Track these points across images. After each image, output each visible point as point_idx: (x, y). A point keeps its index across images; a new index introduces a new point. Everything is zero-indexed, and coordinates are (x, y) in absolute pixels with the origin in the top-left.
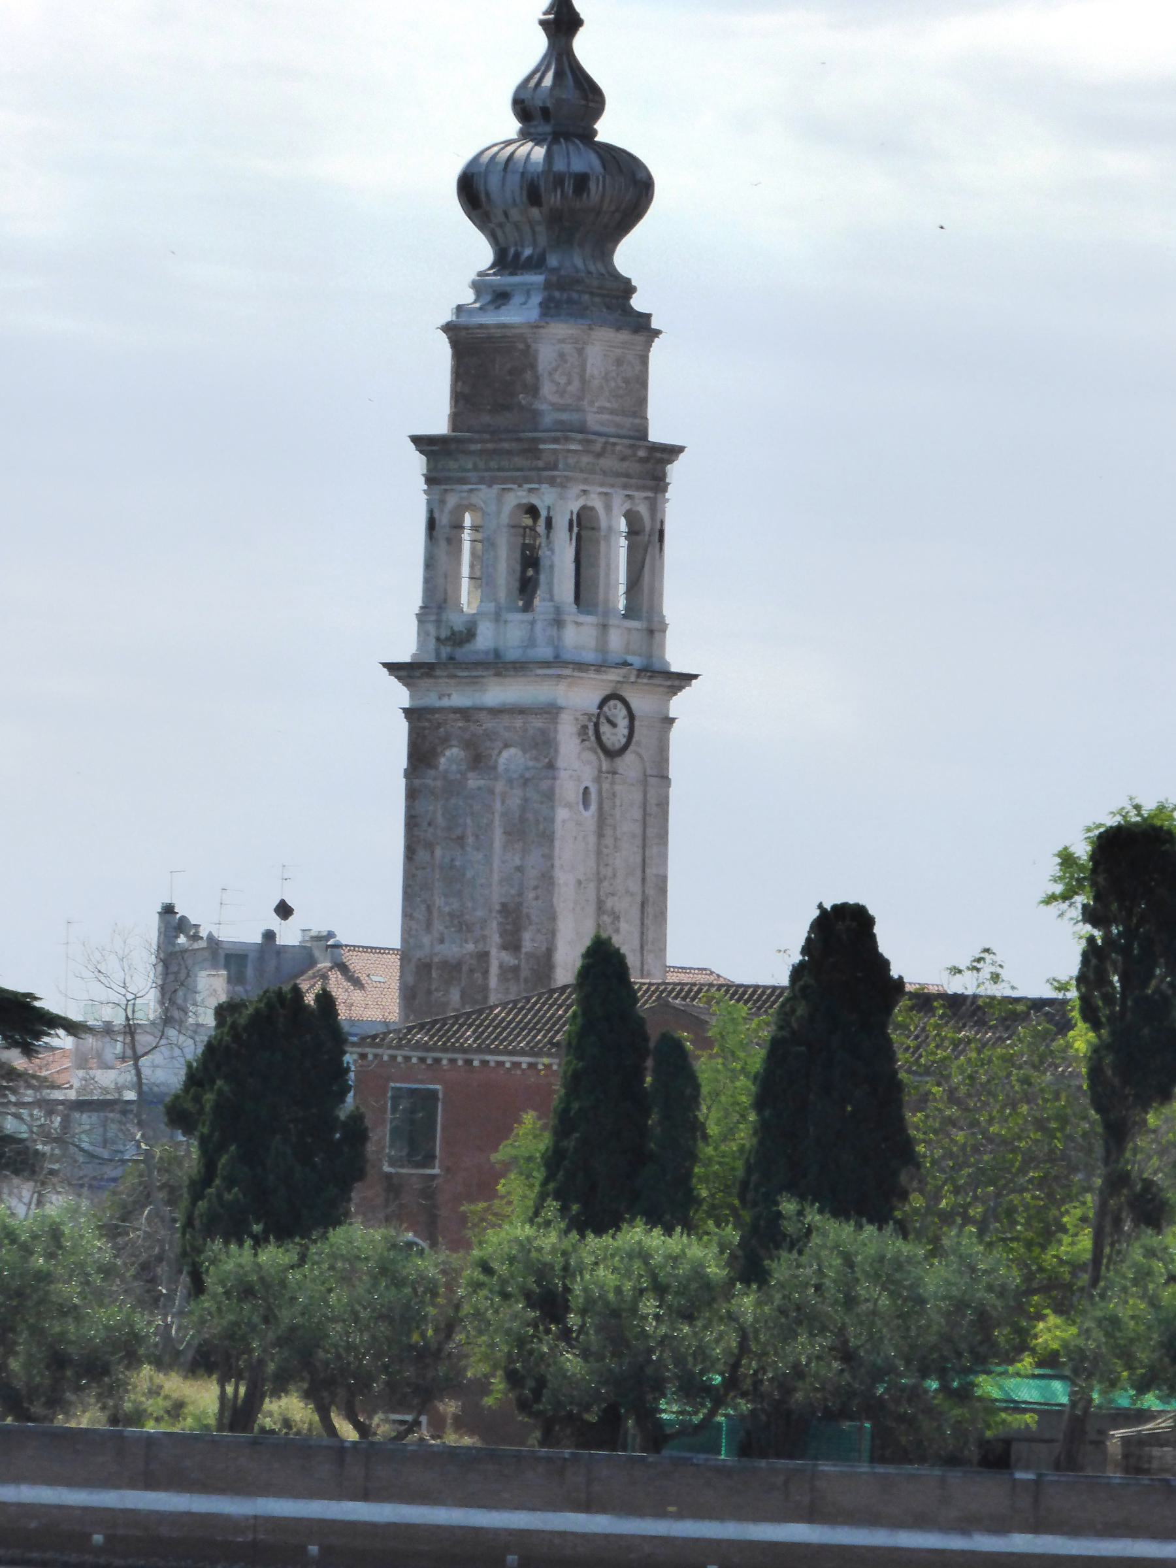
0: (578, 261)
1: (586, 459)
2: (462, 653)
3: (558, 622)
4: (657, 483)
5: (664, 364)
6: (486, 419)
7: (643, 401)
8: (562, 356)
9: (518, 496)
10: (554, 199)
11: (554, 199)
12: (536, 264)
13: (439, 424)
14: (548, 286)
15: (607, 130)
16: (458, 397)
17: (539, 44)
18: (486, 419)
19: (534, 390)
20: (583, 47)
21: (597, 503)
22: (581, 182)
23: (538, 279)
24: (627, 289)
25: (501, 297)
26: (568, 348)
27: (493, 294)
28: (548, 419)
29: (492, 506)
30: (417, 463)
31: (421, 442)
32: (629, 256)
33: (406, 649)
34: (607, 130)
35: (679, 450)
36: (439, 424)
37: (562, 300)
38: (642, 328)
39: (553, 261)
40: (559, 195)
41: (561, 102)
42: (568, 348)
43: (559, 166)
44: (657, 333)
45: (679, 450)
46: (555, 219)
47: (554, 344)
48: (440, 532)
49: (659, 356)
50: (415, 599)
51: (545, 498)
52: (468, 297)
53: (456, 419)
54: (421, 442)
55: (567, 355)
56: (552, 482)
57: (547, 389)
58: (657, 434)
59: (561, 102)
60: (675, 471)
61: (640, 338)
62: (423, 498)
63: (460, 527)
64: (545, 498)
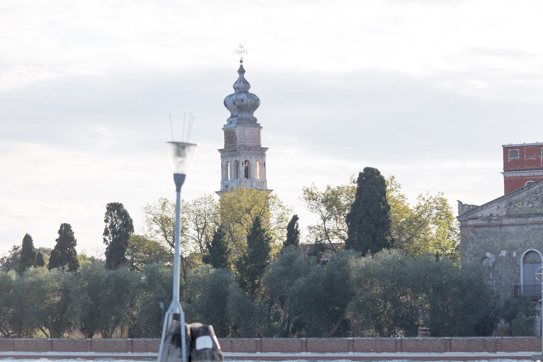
0: (244, 115)
1: (245, 151)
2: (228, 189)
5: (263, 133)
6: (229, 145)
7: (259, 140)
8: (240, 133)
9: (234, 159)
10: (238, 104)
11: (238, 104)
12: (237, 116)
13: (223, 147)
14: (238, 120)
15: (250, 91)
16: (226, 142)
17: (237, 76)
18: (229, 145)
19: (236, 139)
20: (246, 76)
21: (250, 159)
22: (242, 100)
23: (236, 119)
24: (255, 120)
25: (231, 122)
26: (241, 131)
27: (230, 122)
28: (238, 144)
30: (219, 154)
31: (220, 150)
32: (256, 114)
33: (219, 189)
34: (250, 91)
35: (268, 148)
36: (223, 147)
37: (241, 122)
38: (259, 127)
39: (239, 115)
40: (243, 104)
41: (242, 86)
42: (241, 131)
43: (238, 97)
44: (261, 127)
45: (268, 148)
46: (239, 107)
47: (238, 131)
48: (224, 168)
49: (262, 132)
50: (220, 179)
51: (238, 158)
52: (226, 123)
54: (220, 150)
55: (242, 133)
56: (239, 156)
57: (238, 139)
58: (263, 145)
59: (242, 86)
60: (267, 153)
61: (257, 129)
62: (220, 161)
63: (228, 166)
64: (238, 158)
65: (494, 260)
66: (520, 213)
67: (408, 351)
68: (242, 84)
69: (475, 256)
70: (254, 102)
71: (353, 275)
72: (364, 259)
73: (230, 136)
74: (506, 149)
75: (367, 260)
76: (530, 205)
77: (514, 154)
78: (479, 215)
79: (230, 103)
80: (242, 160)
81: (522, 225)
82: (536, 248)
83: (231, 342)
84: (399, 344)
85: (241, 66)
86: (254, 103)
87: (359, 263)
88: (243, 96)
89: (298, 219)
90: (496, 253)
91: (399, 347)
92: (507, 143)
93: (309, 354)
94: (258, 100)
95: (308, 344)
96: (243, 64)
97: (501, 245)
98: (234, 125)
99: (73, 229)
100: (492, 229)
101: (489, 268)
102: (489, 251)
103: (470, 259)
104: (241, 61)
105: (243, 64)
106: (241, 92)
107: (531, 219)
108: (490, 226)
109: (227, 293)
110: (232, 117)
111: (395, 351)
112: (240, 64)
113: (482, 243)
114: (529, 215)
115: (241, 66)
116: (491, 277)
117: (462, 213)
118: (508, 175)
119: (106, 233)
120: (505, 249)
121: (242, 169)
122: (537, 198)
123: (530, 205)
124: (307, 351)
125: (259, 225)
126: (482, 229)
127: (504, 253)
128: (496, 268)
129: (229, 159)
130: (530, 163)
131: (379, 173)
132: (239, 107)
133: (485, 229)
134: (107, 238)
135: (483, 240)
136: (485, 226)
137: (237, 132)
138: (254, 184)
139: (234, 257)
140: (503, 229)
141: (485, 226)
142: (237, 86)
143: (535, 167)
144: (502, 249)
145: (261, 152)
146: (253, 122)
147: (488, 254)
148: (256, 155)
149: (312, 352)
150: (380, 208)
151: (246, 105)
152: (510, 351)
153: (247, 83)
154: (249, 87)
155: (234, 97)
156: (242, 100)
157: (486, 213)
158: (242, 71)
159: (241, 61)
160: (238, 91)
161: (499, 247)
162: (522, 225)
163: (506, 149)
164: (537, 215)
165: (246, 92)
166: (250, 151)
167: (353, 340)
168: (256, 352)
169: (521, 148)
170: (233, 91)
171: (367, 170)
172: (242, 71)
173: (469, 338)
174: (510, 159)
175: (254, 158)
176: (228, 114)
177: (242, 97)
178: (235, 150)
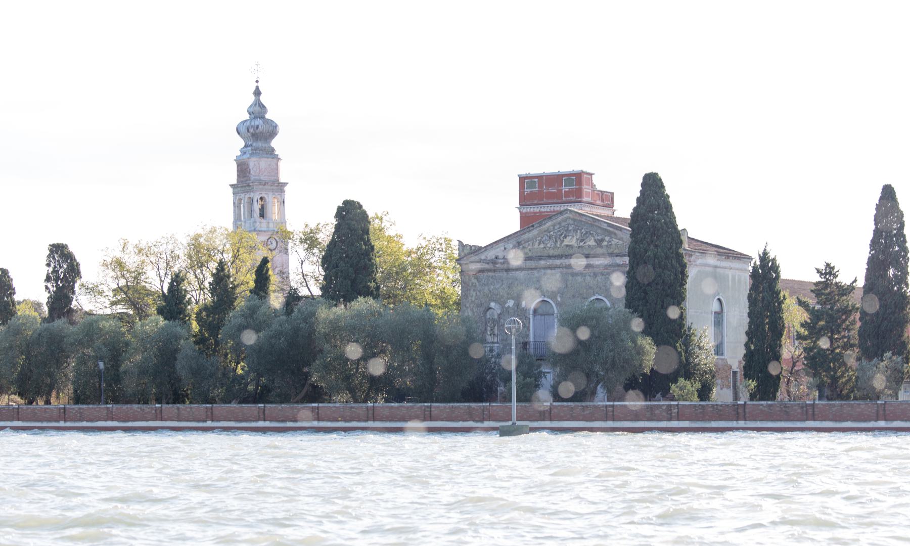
0: (260, 144)
3: (255, 222)
4: (282, 191)
7: (277, 173)
9: (248, 196)
10: (252, 131)
13: (235, 182)
15: (267, 116)
16: (238, 176)
17: (252, 99)
20: (262, 99)
22: (257, 127)
23: (249, 148)
24: (273, 150)
28: (252, 178)
29: (245, 197)
30: (231, 190)
31: (232, 186)
32: (275, 143)
34: (267, 116)
36: (235, 182)
37: (256, 152)
39: (254, 144)
40: (258, 132)
41: (258, 110)
46: (253, 135)
47: (253, 163)
48: (237, 206)
49: (281, 164)
51: (252, 195)
52: (239, 153)
53: (238, 181)
54: (232, 186)
55: (257, 165)
57: (252, 172)
58: (282, 180)
59: (258, 110)
60: (286, 188)
61: (275, 160)
65: (499, 312)
66: (530, 254)
67: (381, 420)
68: (257, 108)
69: (478, 306)
70: (271, 128)
71: (321, 329)
72: (334, 309)
73: (243, 169)
74: (522, 179)
75: (340, 310)
76: (542, 246)
77: (532, 185)
78: (483, 257)
79: (243, 130)
80: (257, 196)
81: (532, 269)
82: (548, 297)
83: (178, 409)
84: (371, 412)
85: (257, 87)
86: (272, 131)
87: (329, 313)
88: (258, 122)
89: (268, 262)
90: (502, 303)
91: (370, 415)
92: (524, 172)
93: (267, 424)
94: (276, 126)
95: (267, 412)
96: (259, 84)
97: (508, 294)
98: (247, 156)
99: (11, 274)
100: (497, 274)
101: (494, 320)
102: (494, 301)
103: (472, 310)
104: (257, 82)
105: (259, 84)
106: (256, 117)
107: (543, 262)
108: (495, 271)
109: (176, 351)
110: (246, 146)
111: (366, 421)
112: (256, 84)
113: (486, 290)
114: (540, 258)
115: (257, 87)
116: (496, 332)
117: (463, 254)
118: (525, 211)
119: (48, 279)
120: (512, 298)
121: (257, 207)
122: (550, 237)
123: (542, 246)
124: (265, 420)
125: (223, 269)
126: (486, 274)
127: (511, 303)
128: (502, 321)
129: (243, 195)
130: (550, 196)
131: (360, 206)
132: (253, 135)
133: (490, 274)
134: (49, 285)
135: (486, 288)
136: (489, 270)
137: (251, 165)
138: (271, 225)
139: (193, 309)
140: (511, 274)
141: (489, 270)
142: (251, 110)
143: (555, 201)
144: (509, 299)
145: (280, 187)
146: (271, 153)
147: (493, 305)
148: (273, 191)
149: (271, 421)
150: (361, 249)
151: (262, 133)
152: (500, 421)
153: (264, 107)
154: (266, 112)
155: (248, 123)
156: (257, 127)
157: (491, 254)
158: (257, 93)
159: (257, 82)
160: (253, 116)
161: (506, 295)
162: (532, 269)
163: (522, 179)
164: (550, 257)
165: (263, 118)
166: (266, 187)
167: (318, 407)
168: (205, 421)
169: (540, 177)
170: (247, 117)
171: (346, 203)
172: (257, 93)
173: (451, 404)
174: (527, 191)
175: (270, 194)
176: (242, 143)
177: (257, 123)
178: (249, 186)
